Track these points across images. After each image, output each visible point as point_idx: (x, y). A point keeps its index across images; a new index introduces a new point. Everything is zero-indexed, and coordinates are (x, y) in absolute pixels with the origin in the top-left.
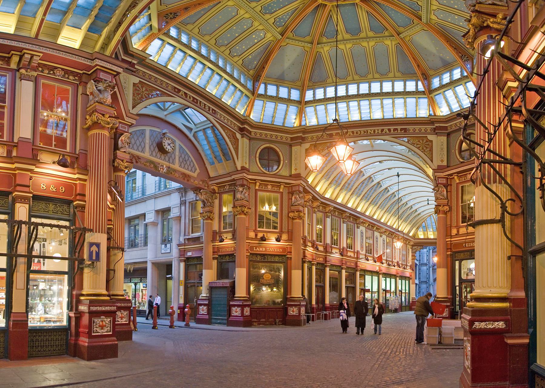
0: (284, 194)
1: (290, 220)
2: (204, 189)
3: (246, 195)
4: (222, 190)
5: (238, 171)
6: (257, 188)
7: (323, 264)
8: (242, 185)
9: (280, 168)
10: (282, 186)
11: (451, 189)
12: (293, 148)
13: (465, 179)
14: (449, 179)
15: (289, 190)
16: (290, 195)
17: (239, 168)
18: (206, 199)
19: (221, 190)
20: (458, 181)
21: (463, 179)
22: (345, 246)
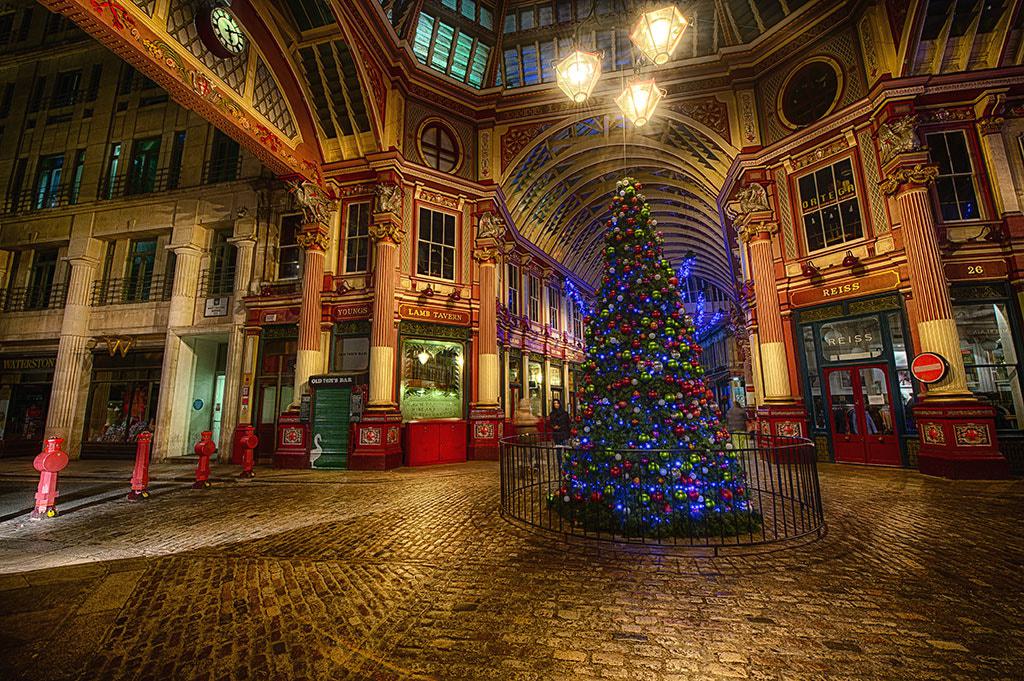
0: (464, 215)
1: (476, 264)
2: (308, 181)
3: (398, 204)
4: (348, 193)
5: (382, 152)
6: (417, 196)
7: (519, 350)
8: (391, 184)
9: (458, 167)
10: (462, 201)
11: (775, 190)
12: (481, 133)
14: (768, 172)
15: (472, 209)
16: (476, 219)
17: (386, 148)
18: (314, 207)
19: (346, 195)
20: (790, 171)
22: (548, 322)
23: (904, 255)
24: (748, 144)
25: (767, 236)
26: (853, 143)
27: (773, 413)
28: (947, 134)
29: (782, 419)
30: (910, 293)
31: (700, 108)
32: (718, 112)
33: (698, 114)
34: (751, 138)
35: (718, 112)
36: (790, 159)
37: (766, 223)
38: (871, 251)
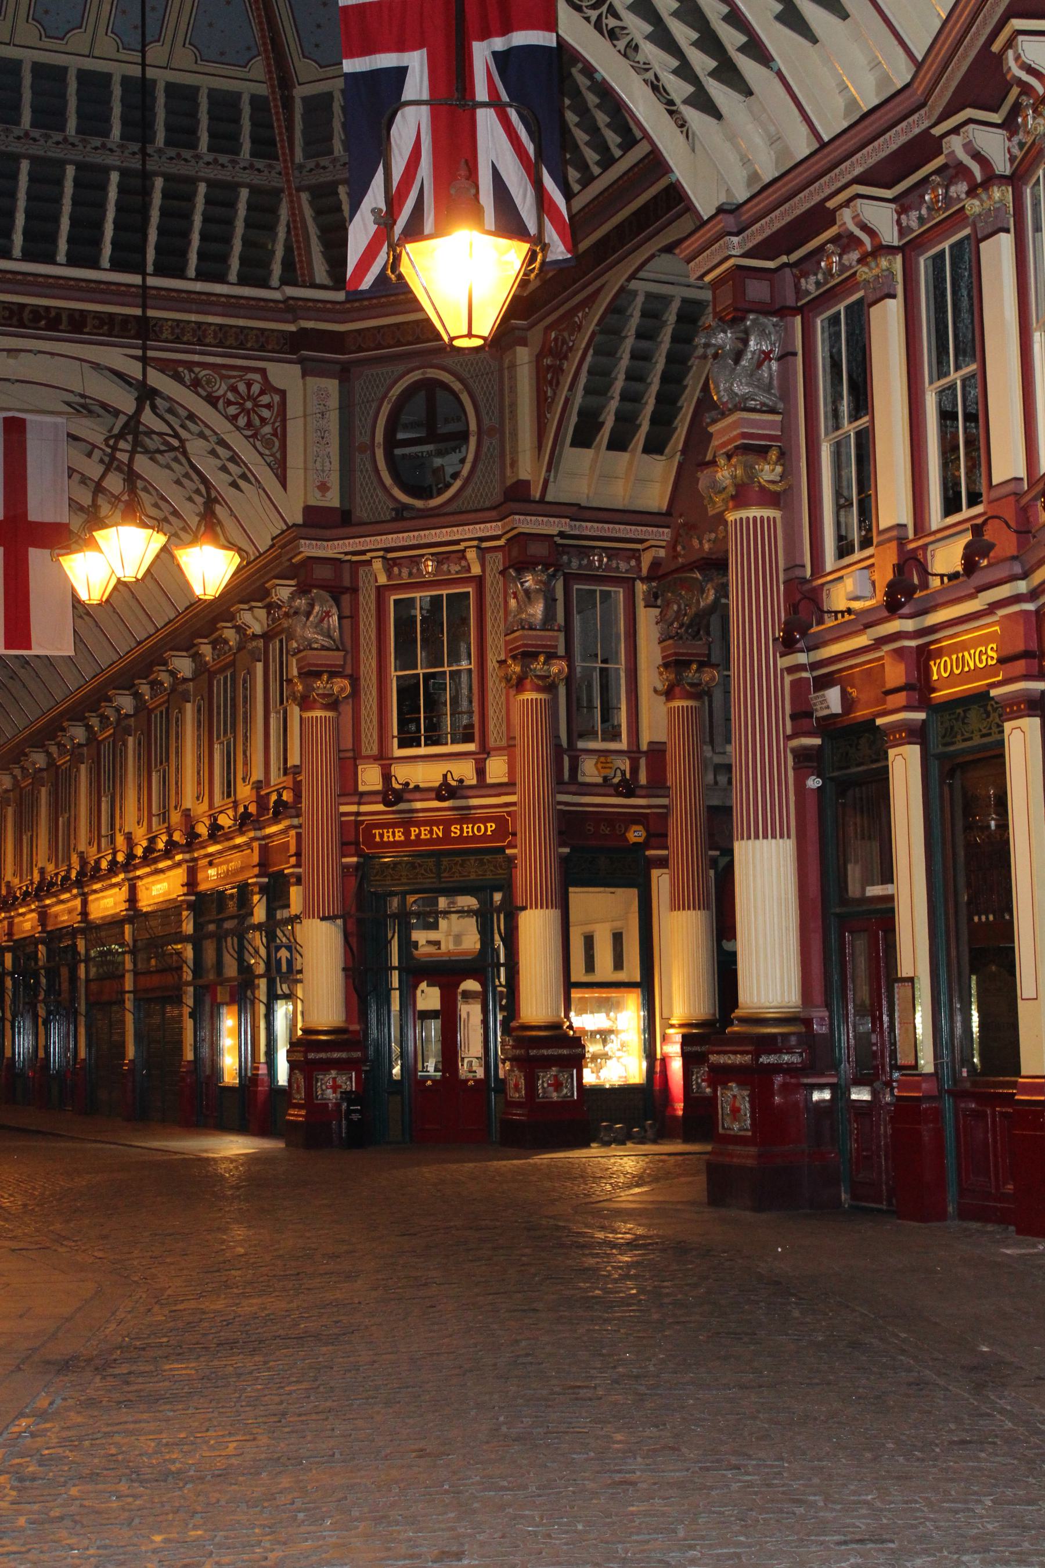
13: (410, 574)
20: (383, 580)
21: (405, 572)
23: (514, 793)
24: (316, 500)
25: (333, 704)
26: (476, 570)
27: (311, 1056)
28: (601, 591)
29: (326, 1065)
30: (515, 857)
31: (234, 389)
32: (268, 406)
33: (229, 403)
34: (323, 488)
35: (268, 406)
36: (383, 557)
37: (333, 675)
38: (481, 772)
